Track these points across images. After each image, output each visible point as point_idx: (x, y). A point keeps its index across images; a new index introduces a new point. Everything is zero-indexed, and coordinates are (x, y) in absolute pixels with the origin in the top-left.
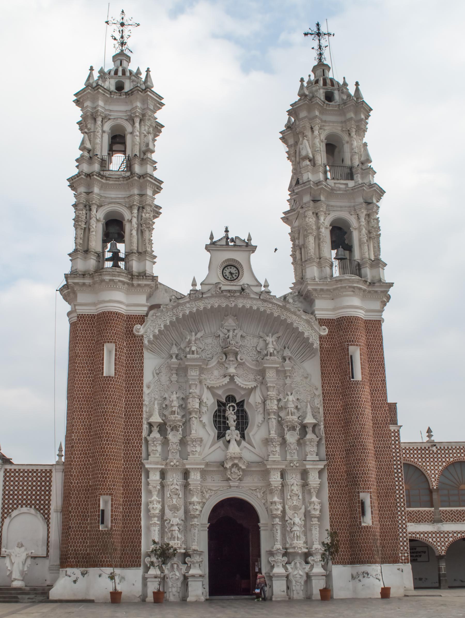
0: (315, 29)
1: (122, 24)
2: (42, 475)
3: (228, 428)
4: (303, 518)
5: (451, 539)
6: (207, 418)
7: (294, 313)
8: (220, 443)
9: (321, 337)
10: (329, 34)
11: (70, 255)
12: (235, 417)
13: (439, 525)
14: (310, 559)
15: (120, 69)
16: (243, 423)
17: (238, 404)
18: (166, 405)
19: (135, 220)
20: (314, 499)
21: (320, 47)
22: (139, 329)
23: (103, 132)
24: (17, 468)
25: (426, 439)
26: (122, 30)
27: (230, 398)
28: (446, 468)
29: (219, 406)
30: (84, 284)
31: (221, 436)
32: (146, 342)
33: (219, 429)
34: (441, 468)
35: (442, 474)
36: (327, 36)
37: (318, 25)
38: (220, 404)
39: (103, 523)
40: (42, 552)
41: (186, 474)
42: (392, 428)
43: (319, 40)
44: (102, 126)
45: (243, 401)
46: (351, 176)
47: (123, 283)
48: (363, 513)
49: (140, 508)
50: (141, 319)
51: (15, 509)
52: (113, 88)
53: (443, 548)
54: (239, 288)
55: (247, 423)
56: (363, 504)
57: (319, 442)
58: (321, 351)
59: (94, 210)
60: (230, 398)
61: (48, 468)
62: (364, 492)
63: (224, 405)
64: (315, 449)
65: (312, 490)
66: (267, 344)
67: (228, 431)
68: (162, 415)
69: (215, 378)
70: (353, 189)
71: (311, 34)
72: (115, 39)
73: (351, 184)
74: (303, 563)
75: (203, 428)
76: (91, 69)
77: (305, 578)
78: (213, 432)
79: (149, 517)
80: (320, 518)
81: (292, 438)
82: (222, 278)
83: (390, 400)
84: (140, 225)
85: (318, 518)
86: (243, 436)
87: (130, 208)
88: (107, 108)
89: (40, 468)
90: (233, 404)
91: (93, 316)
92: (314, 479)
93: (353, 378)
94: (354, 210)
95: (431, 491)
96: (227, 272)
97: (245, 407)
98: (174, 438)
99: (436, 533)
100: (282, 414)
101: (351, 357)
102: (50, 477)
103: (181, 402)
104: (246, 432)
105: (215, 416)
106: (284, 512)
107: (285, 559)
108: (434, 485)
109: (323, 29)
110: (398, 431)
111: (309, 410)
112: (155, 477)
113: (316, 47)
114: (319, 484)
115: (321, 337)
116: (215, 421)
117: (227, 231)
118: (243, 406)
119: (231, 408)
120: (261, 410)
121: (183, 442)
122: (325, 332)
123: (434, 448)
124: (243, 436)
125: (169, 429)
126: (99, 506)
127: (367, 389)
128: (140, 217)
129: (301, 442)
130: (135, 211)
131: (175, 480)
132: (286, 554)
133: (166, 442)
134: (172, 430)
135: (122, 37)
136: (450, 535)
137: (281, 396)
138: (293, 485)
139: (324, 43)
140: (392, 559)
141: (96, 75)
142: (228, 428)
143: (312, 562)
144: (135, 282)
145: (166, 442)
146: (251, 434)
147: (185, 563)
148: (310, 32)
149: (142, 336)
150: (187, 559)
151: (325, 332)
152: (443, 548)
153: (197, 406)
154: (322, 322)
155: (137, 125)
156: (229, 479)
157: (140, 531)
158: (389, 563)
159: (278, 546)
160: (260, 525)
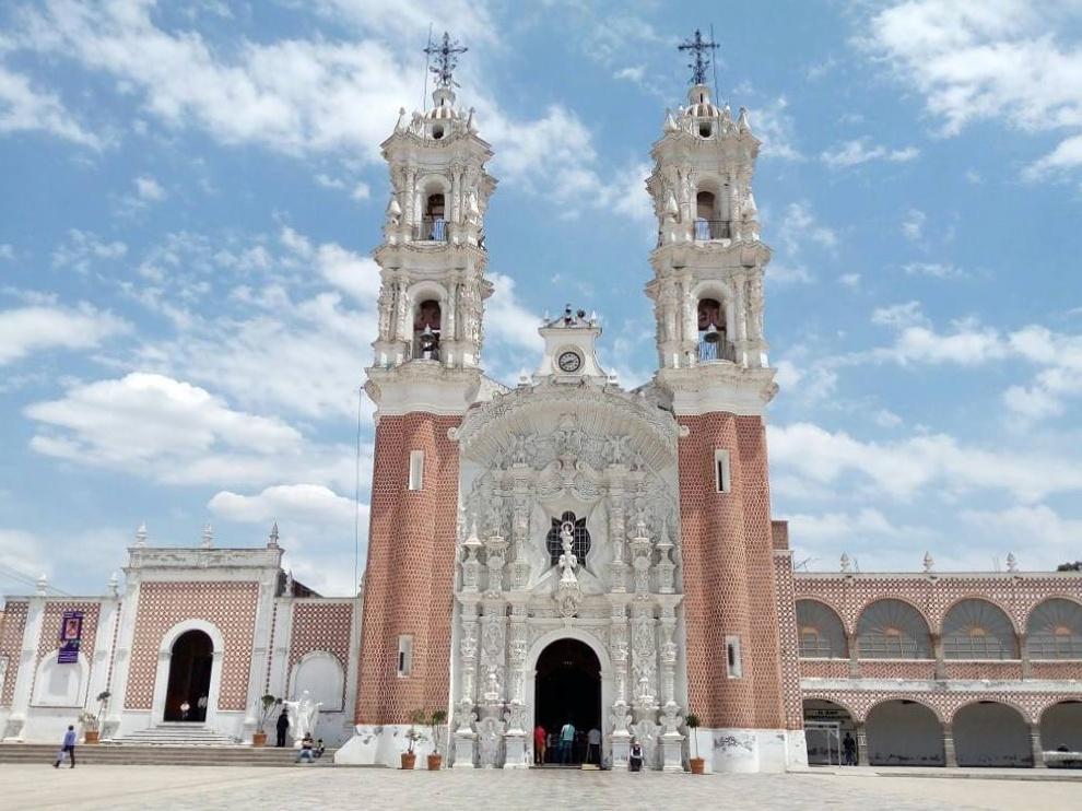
0: (694, 40)
1: (446, 51)
2: (341, 610)
3: (563, 552)
4: (655, 666)
5: (873, 701)
6: (540, 540)
8: (554, 569)
9: (680, 439)
10: (713, 46)
11: (373, 345)
12: (572, 539)
13: (856, 681)
14: (662, 719)
15: (440, 109)
16: (582, 546)
17: (577, 524)
18: (488, 525)
19: (452, 301)
20: (669, 643)
21: (699, 63)
22: (454, 434)
23: (416, 192)
24: (326, 602)
26: (446, 60)
27: (568, 516)
28: (867, 607)
29: (554, 524)
30: (388, 380)
31: (555, 562)
33: (553, 553)
34: (860, 606)
35: (862, 614)
36: (709, 50)
37: (698, 33)
38: (556, 523)
39: (401, 668)
40: (337, 704)
41: (509, 610)
42: (781, 553)
43: (699, 55)
44: (414, 185)
45: (585, 519)
46: (728, 234)
48: (732, 662)
49: (449, 651)
50: (457, 421)
51: (307, 652)
52: (430, 135)
53: (862, 712)
54: (578, 380)
55: (588, 547)
56: (731, 650)
57: (675, 571)
58: (680, 456)
59: (403, 293)
60: (568, 516)
61: (347, 602)
62: (731, 634)
63: (561, 523)
64: (671, 579)
65: (666, 631)
66: (613, 449)
67: (562, 556)
70: (729, 250)
71: (688, 47)
72: (436, 71)
73: (726, 243)
74: (653, 724)
75: (532, 555)
76: (402, 112)
77: (655, 744)
78: (544, 558)
79: (461, 663)
80: (676, 668)
81: (642, 563)
82: (558, 369)
83: (775, 517)
84: (457, 307)
85: (674, 667)
86: (582, 562)
87: (447, 287)
88: (421, 160)
89: (337, 602)
90: (569, 523)
91: (399, 419)
92: (668, 620)
93: (721, 489)
94: (729, 277)
95: (846, 636)
96: (565, 360)
97: (587, 527)
98: (495, 563)
100: (630, 535)
101: (720, 464)
102: (350, 613)
103: (506, 520)
104: (586, 557)
105: (549, 537)
106: (630, 658)
107: (630, 718)
108: (851, 628)
109: (705, 39)
110: (790, 557)
111: (664, 529)
112: (470, 616)
113: (694, 64)
114: (676, 624)
115: (680, 439)
116: (549, 544)
118: (584, 525)
119: (567, 528)
120: (604, 530)
121: (505, 570)
122: (685, 432)
123: (851, 581)
124: (582, 562)
125: (489, 556)
126: (398, 649)
127: (739, 503)
128: (458, 298)
129: (652, 571)
130: (453, 289)
131: (494, 619)
132: (631, 712)
133: (485, 571)
134: (493, 555)
135: (445, 67)
136: (872, 695)
137: (630, 513)
138: (641, 624)
139: (704, 57)
140: (769, 722)
141: (408, 119)
142: (563, 552)
143: (664, 724)
145: (485, 571)
146: (591, 561)
147: (504, 720)
148: (687, 44)
149: (458, 441)
150: (506, 716)
151: (685, 432)
152: (862, 712)
153: (524, 525)
154: (682, 420)
155: (457, 180)
156: (561, 616)
157: (448, 679)
158: (766, 727)
159: (622, 701)
160: (601, 673)
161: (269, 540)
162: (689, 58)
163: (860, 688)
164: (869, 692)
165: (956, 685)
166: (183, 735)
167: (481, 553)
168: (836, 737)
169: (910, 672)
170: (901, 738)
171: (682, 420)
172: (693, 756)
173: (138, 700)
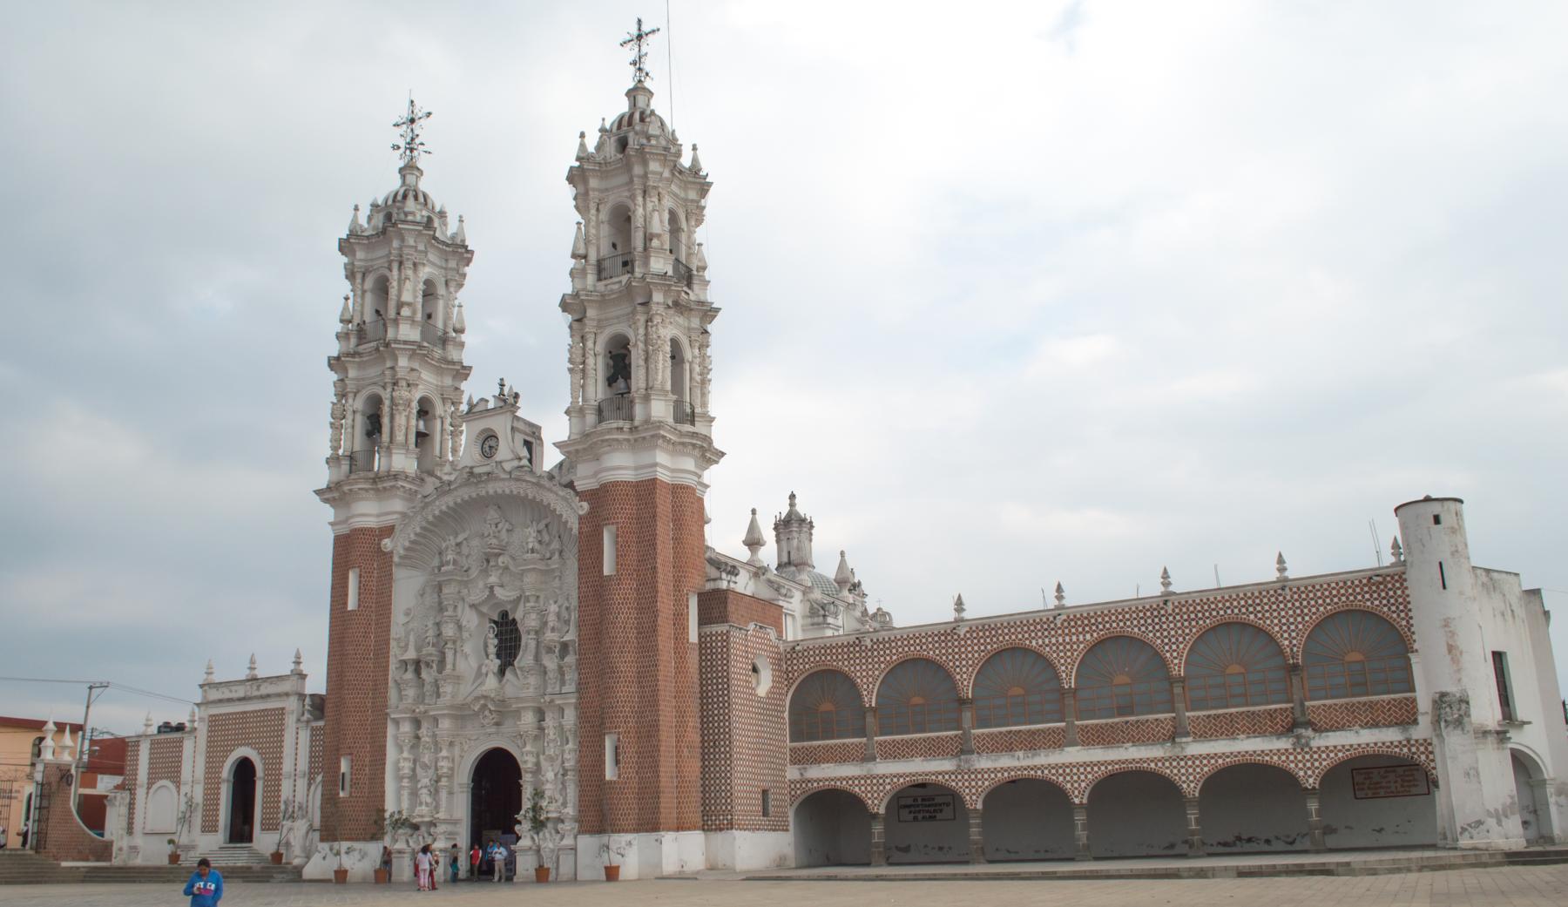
7: (550, 490)
9: (580, 518)
13: (870, 765)
22: (387, 543)
25: (1052, 603)
32: (396, 559)
47: (366, 490)
50: (388, 531)
68: (418, 649)
69: (477, 594)
87: (384, 387)
99: (865, 778)
115: (580, 518)
117: (502, 385)
144: (380, 486)
154: (582, 495)
161: (292, 666)
162: (630, 53)
163: (877, 773)
164: (884, 776)
165: (983, 763)
166: (239, 857)
167: (417, 665)
168: (834, 830)
169: (933, 750)
170: (924, 825)
171: (582, 495)
172: (332, 876)
173: (209, 827)
